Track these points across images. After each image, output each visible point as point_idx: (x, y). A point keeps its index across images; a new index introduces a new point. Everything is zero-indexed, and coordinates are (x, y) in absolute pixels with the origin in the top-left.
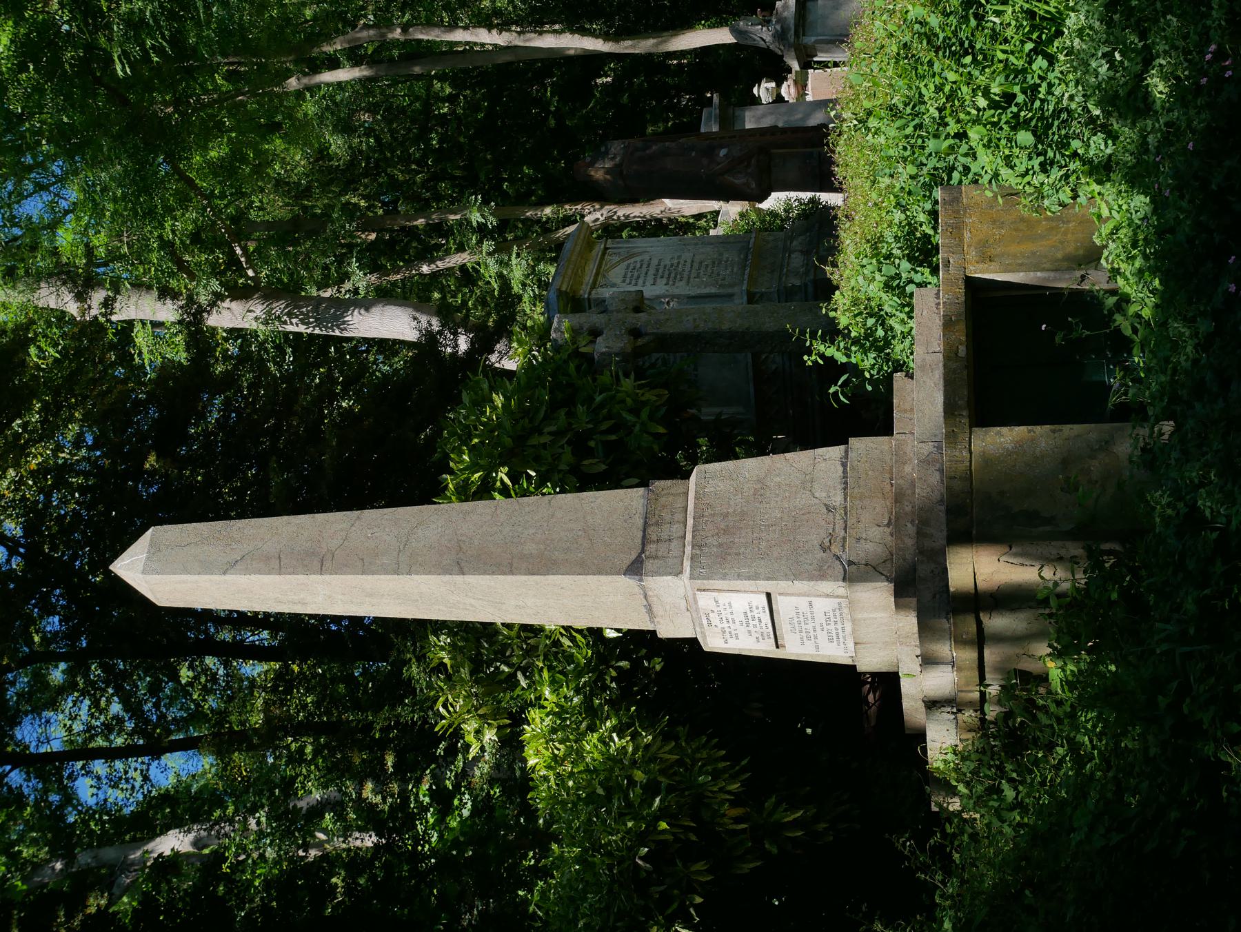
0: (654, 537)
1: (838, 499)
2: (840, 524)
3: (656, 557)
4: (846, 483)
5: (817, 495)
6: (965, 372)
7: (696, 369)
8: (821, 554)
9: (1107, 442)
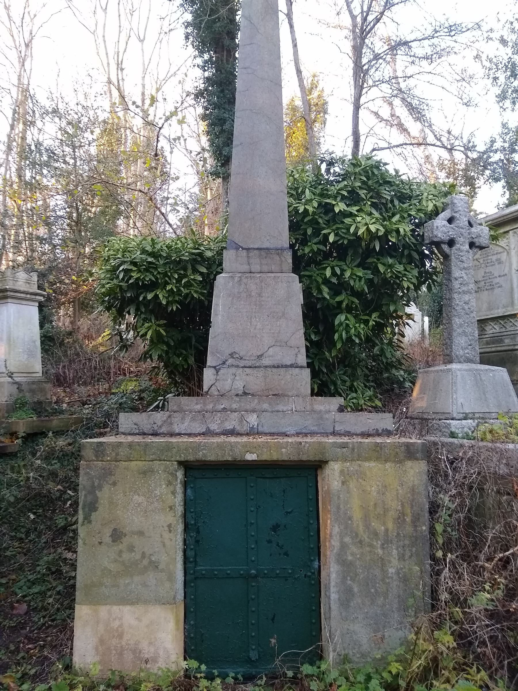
0: (251, 254)
1: (266, 362)
2: (249, 363)
3: (237, 256)
4: (278, 367)
5: (271, 349)
6: (230, 459)
7: (486, 289)
8: (228, 352)
9: (157, 567)
